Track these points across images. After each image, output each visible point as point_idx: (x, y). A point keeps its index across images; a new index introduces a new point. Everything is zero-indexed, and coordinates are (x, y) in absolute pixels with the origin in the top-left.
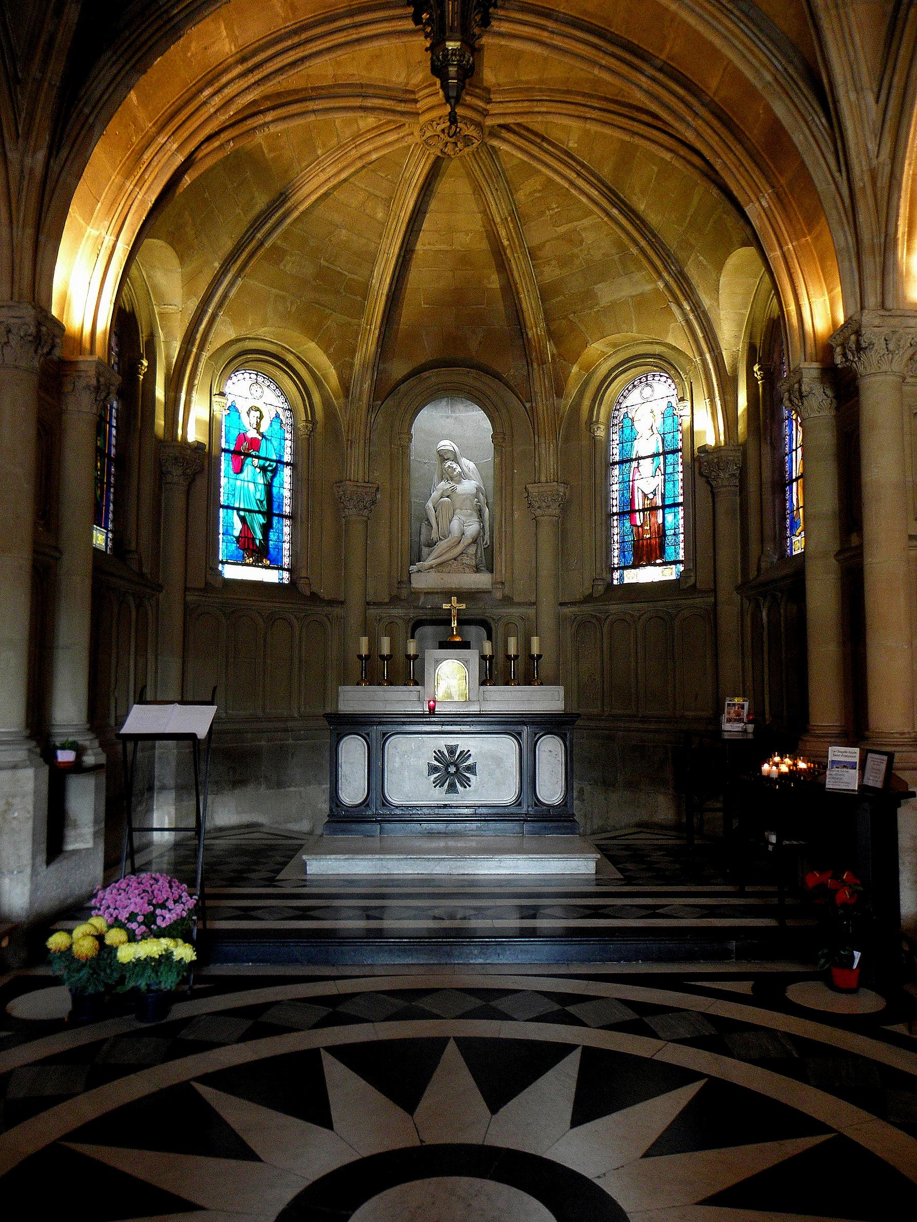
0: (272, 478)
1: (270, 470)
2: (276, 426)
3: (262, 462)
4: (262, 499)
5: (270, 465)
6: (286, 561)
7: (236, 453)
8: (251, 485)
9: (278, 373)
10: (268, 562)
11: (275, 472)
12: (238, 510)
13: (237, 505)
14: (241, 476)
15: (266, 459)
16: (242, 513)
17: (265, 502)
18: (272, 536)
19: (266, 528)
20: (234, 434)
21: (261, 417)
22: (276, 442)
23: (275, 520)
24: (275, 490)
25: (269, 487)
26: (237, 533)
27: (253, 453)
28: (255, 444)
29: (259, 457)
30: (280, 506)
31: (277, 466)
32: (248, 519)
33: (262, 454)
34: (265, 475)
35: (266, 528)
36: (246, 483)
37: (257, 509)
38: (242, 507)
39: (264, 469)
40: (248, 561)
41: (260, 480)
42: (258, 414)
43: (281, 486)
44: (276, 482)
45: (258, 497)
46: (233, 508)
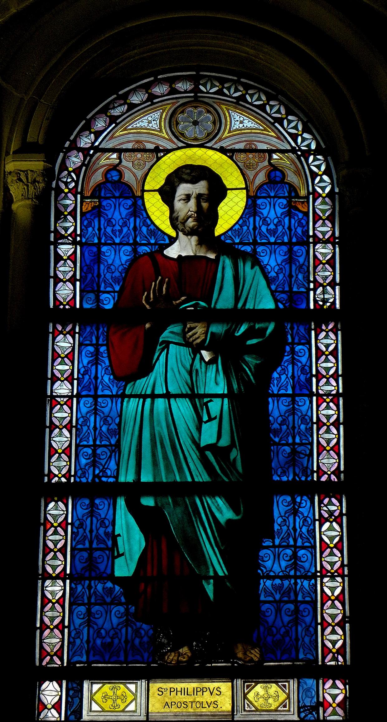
0: (264, 374)
1: (254, 354)
2: (272, 211)
3: (217, 329)
4: (225, 442)
5: (248, 334)
6: (335, 638)
7: (126, 316)
8: (183, 409)
9: (247, 49)
10: (255, 654)
11: (273, 352)
12: (133, 492)
13: (127, 476)
14: (142, 385)
15: (235, 315)
16: (148, 501)
17: (235, 454)
18: (272, 562)
19: (243, 541)
20: (117, 258)
21: (218, 191)
22: (272, 260)
23: (280, 506)
24: (276, 409)
25: (248, 404)
26: (124, 568)
27: (189, 306)
28: (195, 276)
29: (211, 316)
30: (300, 456)
31: (279, 332)
32: (173, 514)
33: (224, 300)
34: (231, 368)
35: (243, 541)
36: (160, 403)
37: (202, 476)
38: (146, 477)
39: (227, 352)
40: (172, 657)
41: (214, 382)
42: (201, 187)
43: (303, 388)
44: (282, 380)
45: (209, 435)
46: (115, 490)
